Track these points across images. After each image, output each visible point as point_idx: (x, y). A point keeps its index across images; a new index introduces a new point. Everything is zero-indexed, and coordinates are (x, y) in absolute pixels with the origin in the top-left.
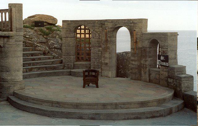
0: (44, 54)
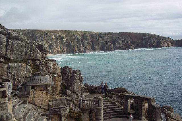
0: (118, 107)
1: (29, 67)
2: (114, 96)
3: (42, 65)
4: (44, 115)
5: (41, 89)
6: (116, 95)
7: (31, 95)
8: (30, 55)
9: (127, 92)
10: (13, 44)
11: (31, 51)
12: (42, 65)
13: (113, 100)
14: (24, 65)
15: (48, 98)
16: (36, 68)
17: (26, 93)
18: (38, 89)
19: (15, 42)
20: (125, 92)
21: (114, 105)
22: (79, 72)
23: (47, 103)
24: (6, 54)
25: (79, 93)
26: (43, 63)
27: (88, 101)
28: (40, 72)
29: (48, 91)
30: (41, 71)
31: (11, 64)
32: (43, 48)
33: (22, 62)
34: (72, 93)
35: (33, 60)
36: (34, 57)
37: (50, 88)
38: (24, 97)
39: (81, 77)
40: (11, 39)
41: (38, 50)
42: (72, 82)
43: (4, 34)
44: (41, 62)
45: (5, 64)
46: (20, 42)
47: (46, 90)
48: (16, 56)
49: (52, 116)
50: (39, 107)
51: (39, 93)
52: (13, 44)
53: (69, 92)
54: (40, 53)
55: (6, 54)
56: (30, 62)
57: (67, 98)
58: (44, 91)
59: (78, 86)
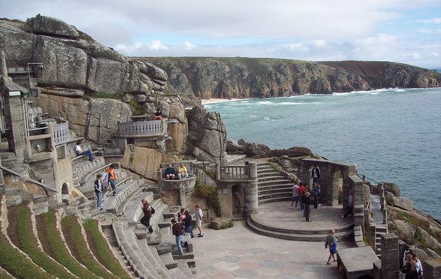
0: (292, 182)
1: (126, 106)
2: (287, 163)
3: (151, 102)
4: (149, 190)
5: (146, 144)
6: (292, 161)
7: (127, 154)
8: (129, 83)
9: (312, 156)
10: (98, 64)
11: (130, 78)
12: (151, 102)
13: (285, 169)
14: (115, 101)
15: (158, 161)
16: (140, 107)
17: (118, 150)
18: (140, 144)
19: (103, 62)
20: (307, 155)
21: (286, 179)
22: (218, 115)
23: (156, 170)
24: (87, 82)
25: (217, 153)
26: (151, 98)
28: (146, 115)
29: (158, 148)
30: (148, 113)
31: (94, 101)
32: (155, 73)
33: (114, 96)
34: (204, 154)
35: (136, 94)
36: (136, 89)
37: (162, 143)
38: (114, 157)
39: (222, 125)
40: (95, 57)
41: (147, 77)
42: (204, 133)
43: (84, 49)
44: (148, 98)
45: (84, 99)
46: (112, 62)
48: (104, 87)
49: (164, 192)
50: (141, 176)
51: (141, 151)
52: (98, 64)
53: (198, 151)
54: (150, 82)
55: (87, 82)
56: (129, 97)
57: (195, 161)
59: (213, 141)
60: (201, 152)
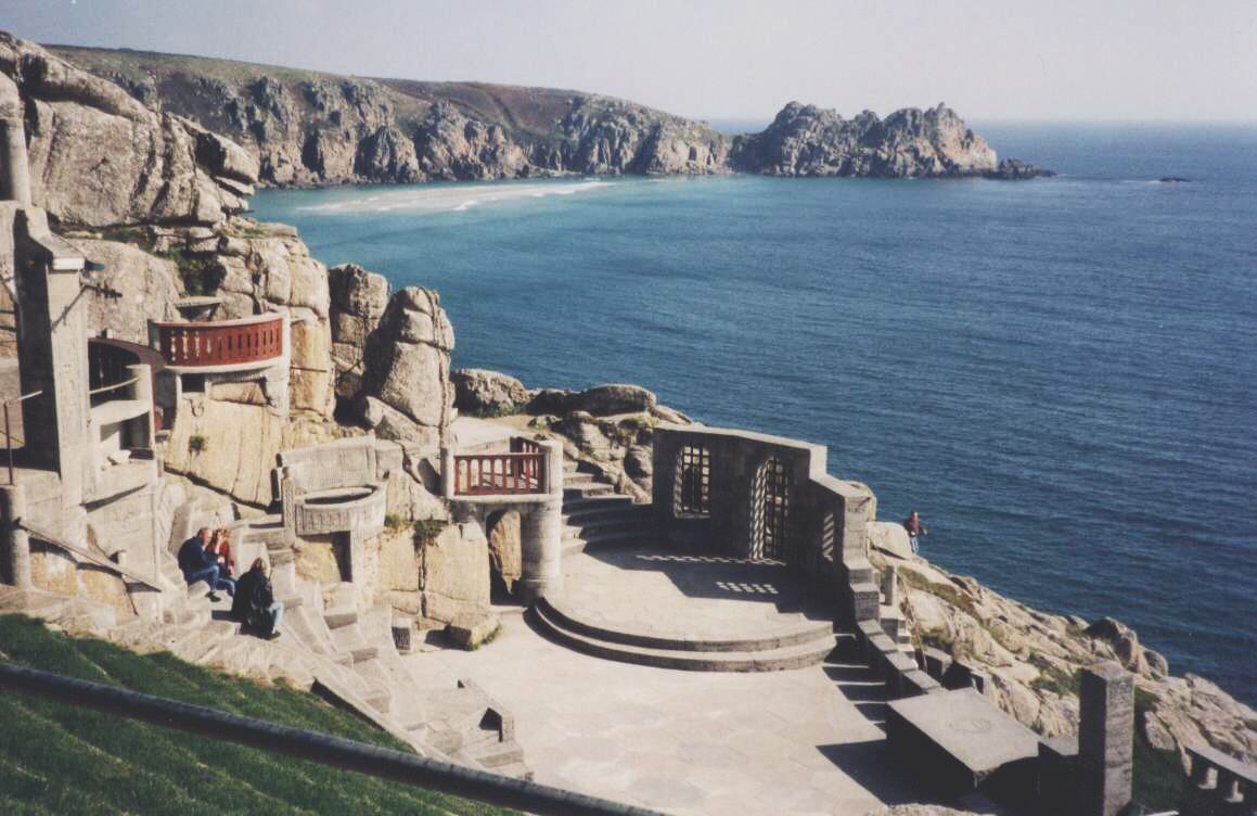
1: (158, 264)
3: (235, 253)
8: (163, 192)
10: (59, 125)
12: (235, 253)
14: (130, 251)
16: (202, 273)
19: (72, 111)
27: (475, 463)
33: (115, 233)
36: (182, 209)
44: (223, 241)
47: (263, 400)
48: (77, 200)
53: (377, 410)
58: (250, 402)
60: (389, 411)
